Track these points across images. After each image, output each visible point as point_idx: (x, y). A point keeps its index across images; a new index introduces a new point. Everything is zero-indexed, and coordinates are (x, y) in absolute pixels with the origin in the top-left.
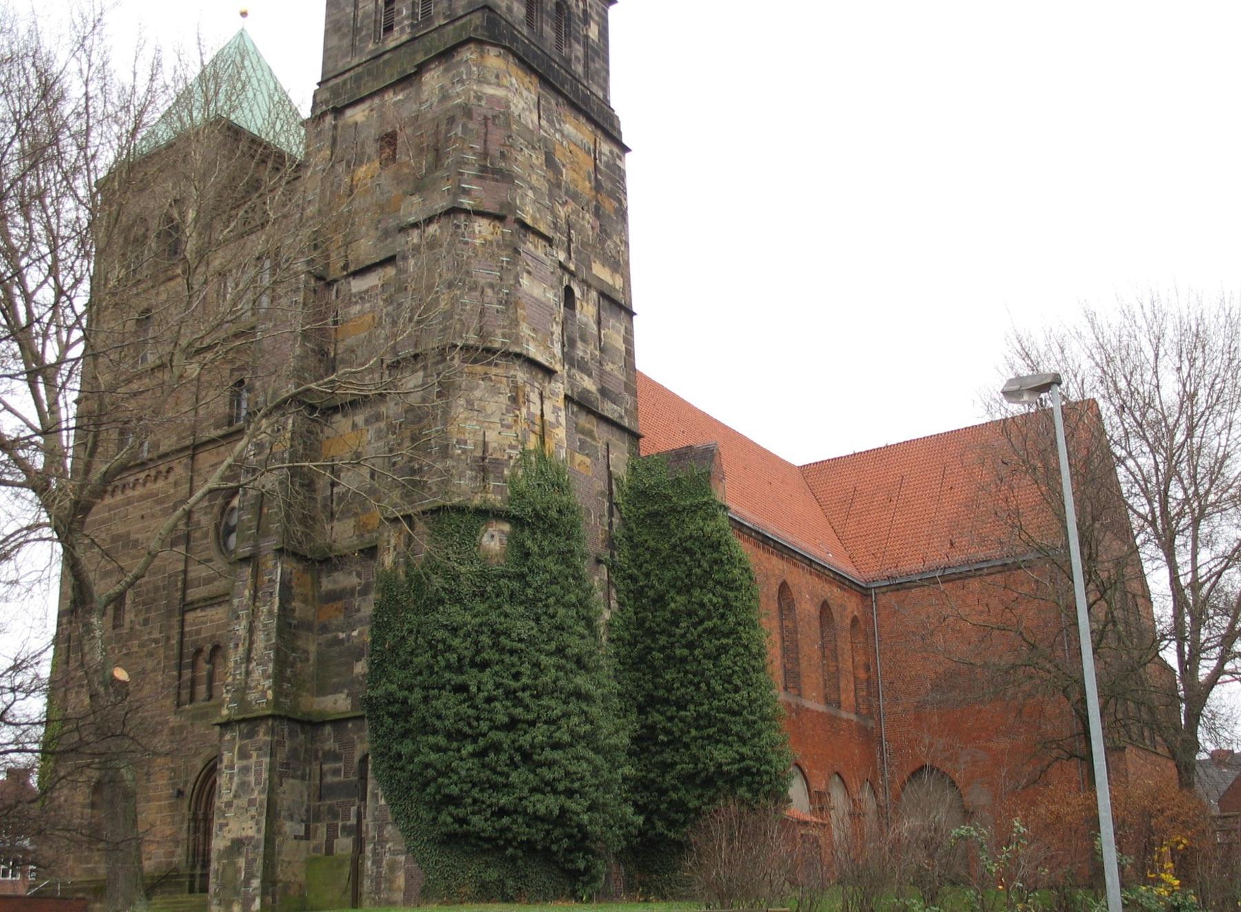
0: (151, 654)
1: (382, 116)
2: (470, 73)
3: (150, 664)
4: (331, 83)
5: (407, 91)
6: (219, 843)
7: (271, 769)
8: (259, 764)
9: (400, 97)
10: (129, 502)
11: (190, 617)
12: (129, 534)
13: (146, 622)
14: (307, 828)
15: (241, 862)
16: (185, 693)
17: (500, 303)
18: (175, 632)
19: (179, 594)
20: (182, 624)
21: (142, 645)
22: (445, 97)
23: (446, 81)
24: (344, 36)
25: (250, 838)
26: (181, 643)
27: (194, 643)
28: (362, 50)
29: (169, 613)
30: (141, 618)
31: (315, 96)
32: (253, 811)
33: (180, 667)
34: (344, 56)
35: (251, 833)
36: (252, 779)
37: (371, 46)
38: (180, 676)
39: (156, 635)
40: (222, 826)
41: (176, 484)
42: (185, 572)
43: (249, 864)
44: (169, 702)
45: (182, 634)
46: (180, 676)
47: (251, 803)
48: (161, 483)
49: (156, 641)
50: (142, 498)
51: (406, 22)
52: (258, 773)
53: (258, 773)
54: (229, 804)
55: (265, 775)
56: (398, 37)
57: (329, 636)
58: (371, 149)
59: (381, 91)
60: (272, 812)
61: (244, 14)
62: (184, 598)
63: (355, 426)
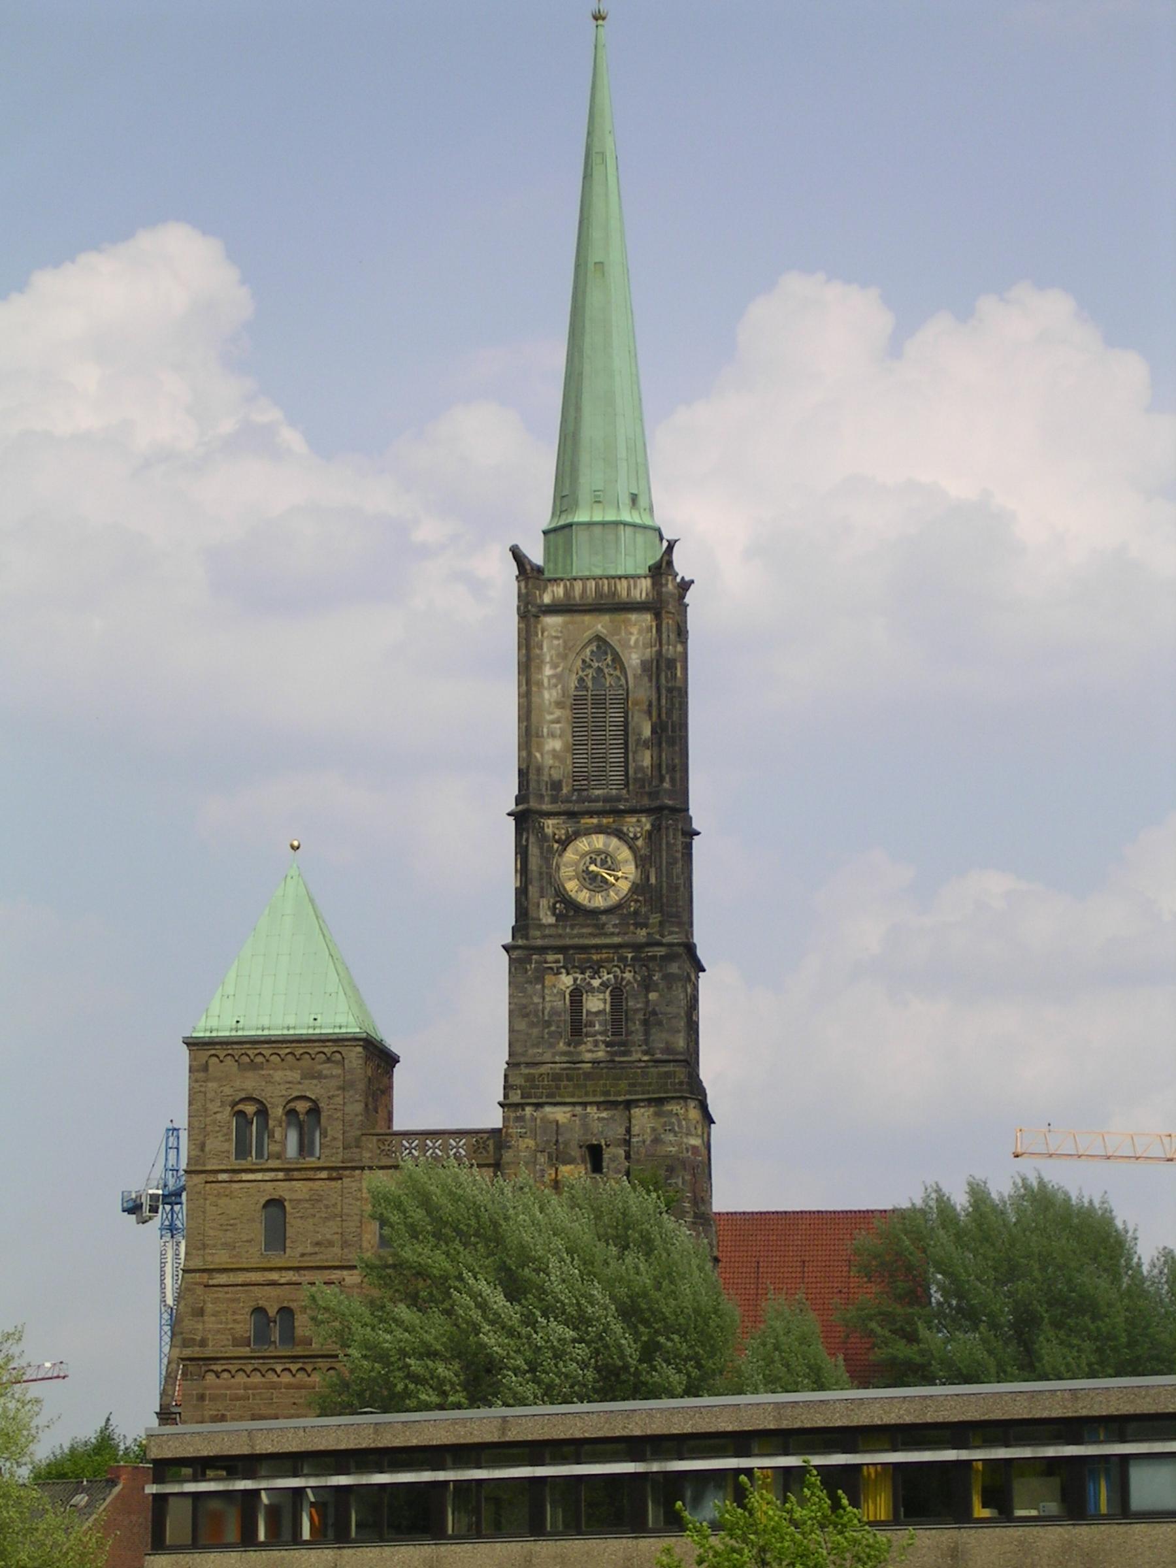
1: (585, 1126)
2: (680, 1126)
5: (611, 1113)
9: (604, 1115)
10: (274, 1386)
22: (657, 1141)
23: (657, 1123)
24: (532, 1025)
28: (552, 1046)
31: (506, 1076)
34: (537, 1045)
37: (561, 1046)
50: (299, 1387)
51: (599, 1038)
56: (592, 1051)
58: (575, 1153)
59: (585, 1105)
61: (295, 848)
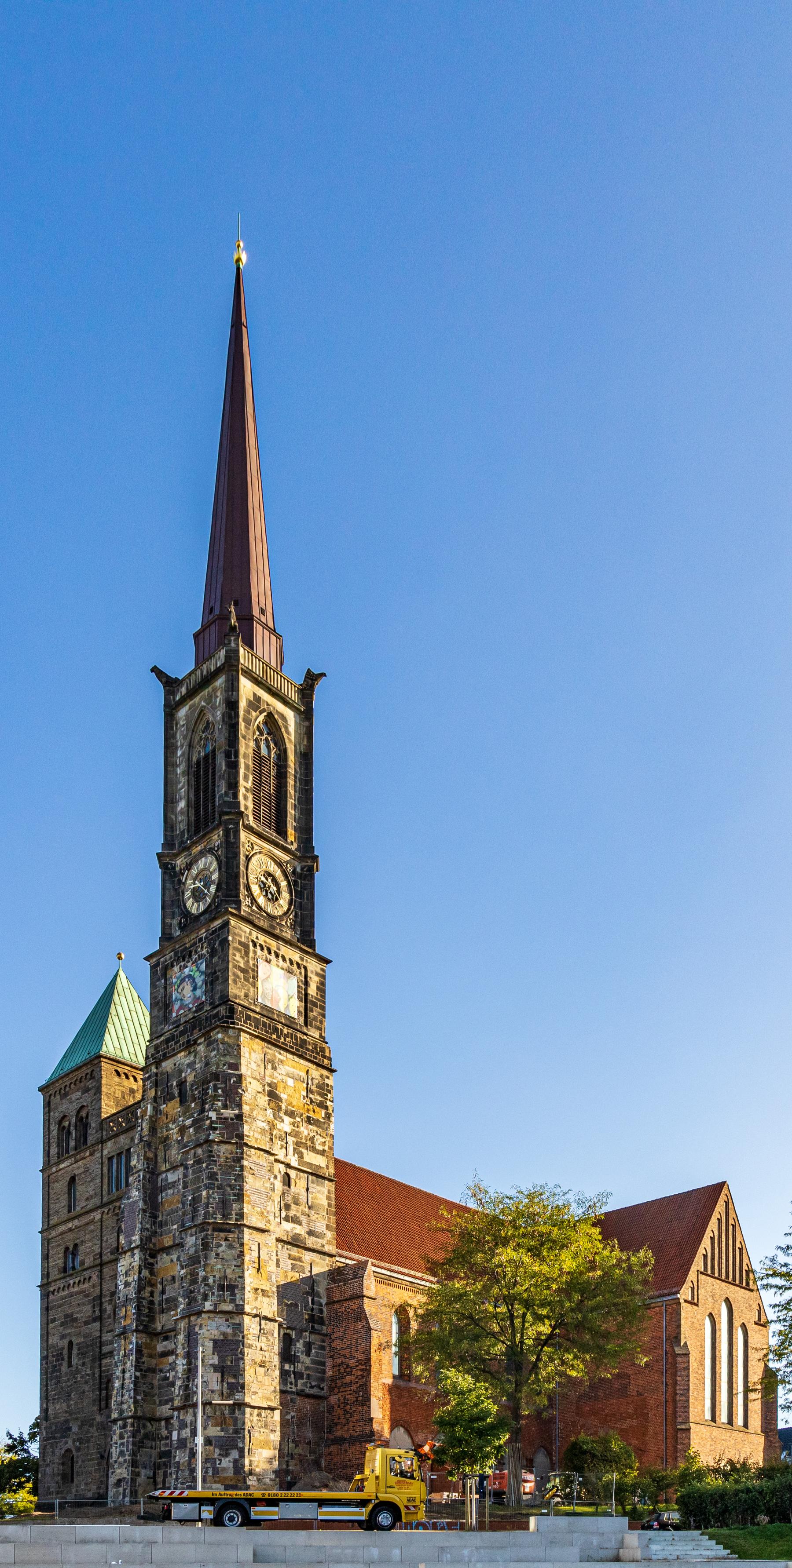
0: (86, 1382)
3: (86, 1388)
4: (155, 1043)
6: (112, 1480)
7: (134, 1444)
8: (128, 1442)
11: (104, 1362)
12: (72, 1313)
13: (84, 1364)
14: (154, 1473)
15: (121, 1490)
16: (103, 1403)
17: (235, 1195)
18: (97, 1370)
19: (97, 1350)
20: (100, 1365)
21: (82, 1377)
25: (124, 1478)
26: (100, 1376)
27: (107, 1376)
29: (93, 1360)
30: (81, 1362)
32: (125, 1465)
33: (100, 1390)
34: (161, 1024)
35: (125, 1476)
36: (125, 1449)
38: (100, 1394)
39: (89, 1372)
40: (113, 1473)
41: (94, 1286)
42: (100, 1337)
43: (124, 1490)
44: (96, 1408)
45: (100, 1371)
46: (100, 1394)
47: (125, 1461)
48: (86, 1285)
49: (88, 1375)
52: (128, 1447)
53: (128, 1447)
54: (116, 1462)
55: (131, 1447)
57: (162, 1375)
60: (134, 1464)
62: (100, 1352)
63: (172, 1261)
